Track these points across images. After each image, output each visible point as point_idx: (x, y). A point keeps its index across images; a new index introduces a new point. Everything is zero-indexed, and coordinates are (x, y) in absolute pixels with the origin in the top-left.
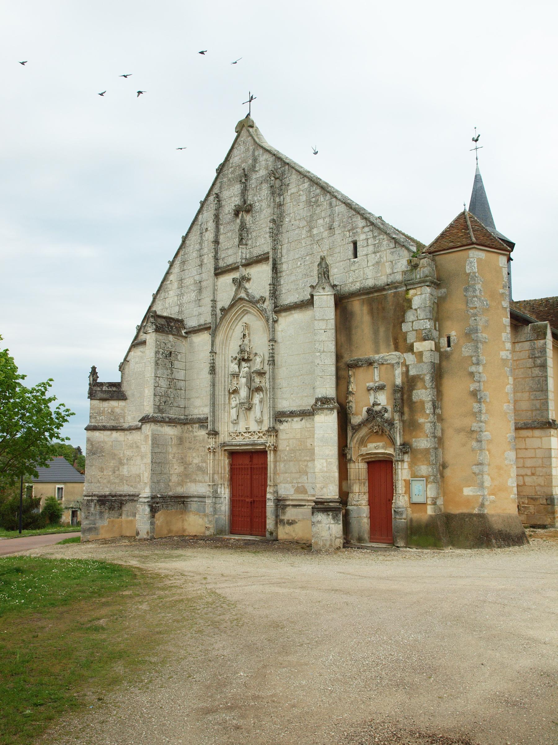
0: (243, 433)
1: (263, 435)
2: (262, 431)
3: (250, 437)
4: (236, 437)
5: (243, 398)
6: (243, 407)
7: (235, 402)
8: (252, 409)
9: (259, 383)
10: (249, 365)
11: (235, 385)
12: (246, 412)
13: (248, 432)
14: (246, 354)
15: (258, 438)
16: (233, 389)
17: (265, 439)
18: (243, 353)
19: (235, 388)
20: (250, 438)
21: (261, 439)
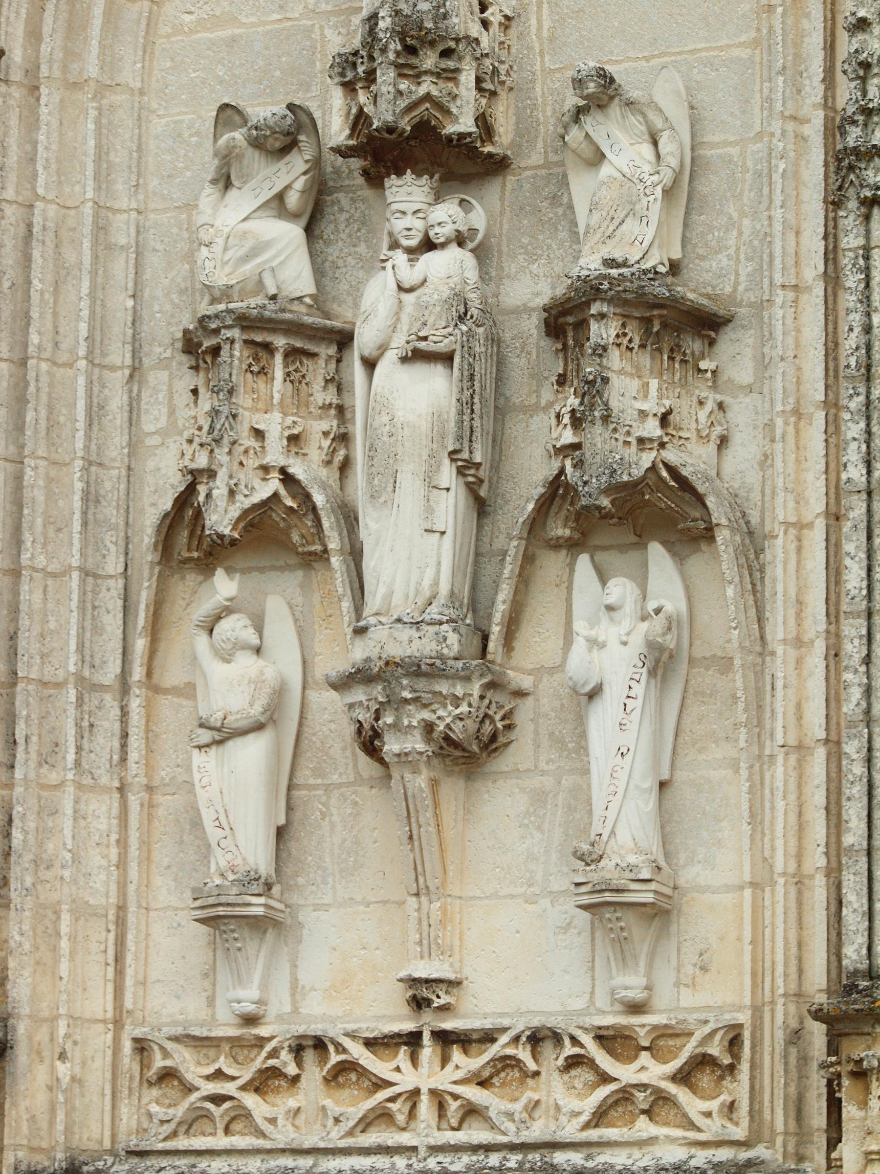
0: (358, 1052)
1: (683, 1077)
2: (663, 1033)
3: (473, 1093)
4: (250, 1100)
5: (402, 607)
6: (417, 716)
7: (246, 662)
8: (505, 761)
9: (652, 429)
10: (478, 219)
11: (275, 455)
12: (434, 784)
13: (444, 1038)
14: (468, 78)
15: (600, 1117)
16: (244, 502)
17: (713, 1128)
18: (429, 60)
19: (274, 485)
20: (471, 1111)
21: (644, 1127)
